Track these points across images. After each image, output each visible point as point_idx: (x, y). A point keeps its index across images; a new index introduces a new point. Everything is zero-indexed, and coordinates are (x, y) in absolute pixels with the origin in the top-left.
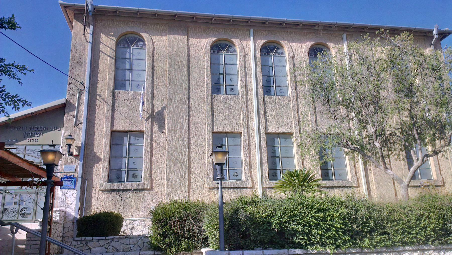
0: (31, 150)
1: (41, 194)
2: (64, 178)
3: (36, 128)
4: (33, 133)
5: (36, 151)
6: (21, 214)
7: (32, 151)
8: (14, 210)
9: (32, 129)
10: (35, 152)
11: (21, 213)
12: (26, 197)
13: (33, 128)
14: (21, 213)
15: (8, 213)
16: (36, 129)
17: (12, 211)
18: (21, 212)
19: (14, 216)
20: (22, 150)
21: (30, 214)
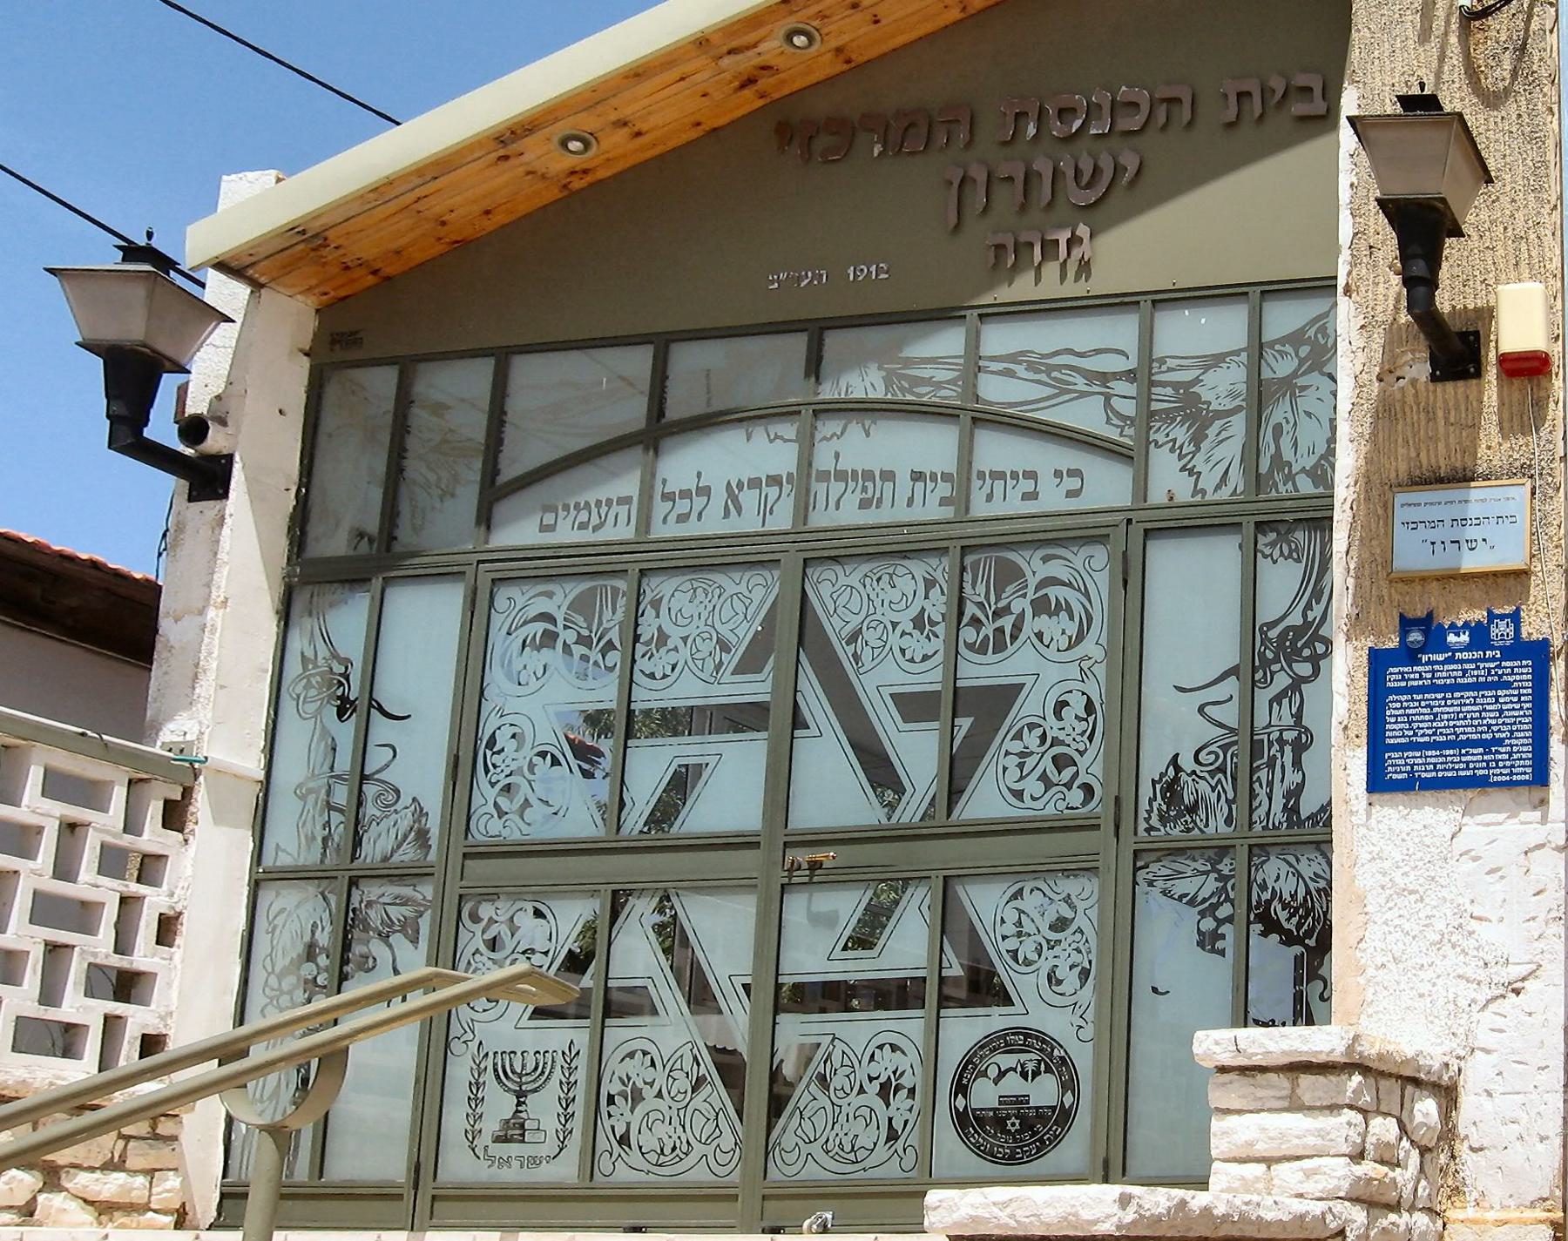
0: (1039, 365)
1: (1178, 875)
2: (1410, 655)
3: (1073, 110)
4: (1043, 166)
5: (1091, 376)
6: (963, 1120)
7: (1050, 369)
8: (886, 1064)
9: (1031, 130)
10: (1080, 383)
11: (960, 1103)
12: (1012, 916)
13: (1042, 113)
14: (960, 1103)
15: (824, 1100)
16: (1077, 124)
17: (862, 1075)
18: (961, 1088)
19: (893, 1136)
20: (942, 375)
21: (1065, 1116)
